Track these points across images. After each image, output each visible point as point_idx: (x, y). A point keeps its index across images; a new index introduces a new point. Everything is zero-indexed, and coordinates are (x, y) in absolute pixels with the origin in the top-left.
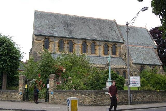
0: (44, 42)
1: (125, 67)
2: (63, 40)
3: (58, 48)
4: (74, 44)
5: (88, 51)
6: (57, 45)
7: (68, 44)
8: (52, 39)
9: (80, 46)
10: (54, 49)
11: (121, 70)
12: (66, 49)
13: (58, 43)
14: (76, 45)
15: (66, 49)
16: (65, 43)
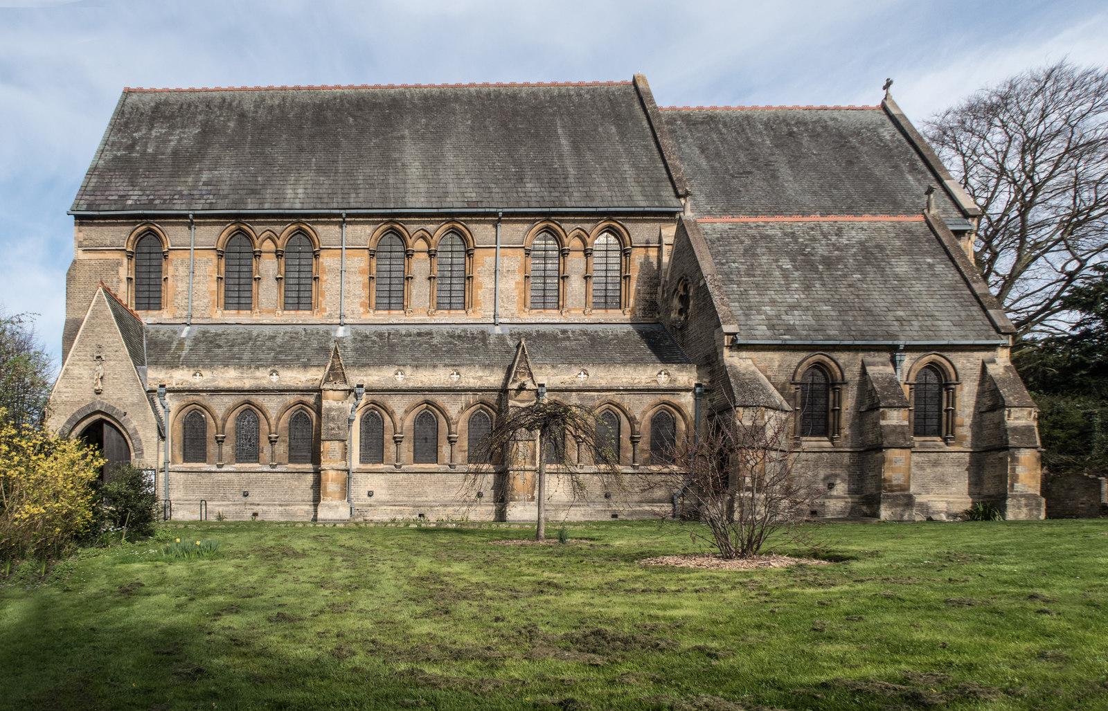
0: (130, 257)
1: (663, 381)
2: (248, 236)
3: (214, 286)
4: (316, 255)
5: (414, 292)
6: (208, 269)
7: (279, 254)
8: (174, 235)
9: (359, 261)
10: (191, 293)
11: (628, 401)
12: (268, 292)
13: (213, 256)
14: (328, 260)
15: (268, 292)
16: (257, 255)
